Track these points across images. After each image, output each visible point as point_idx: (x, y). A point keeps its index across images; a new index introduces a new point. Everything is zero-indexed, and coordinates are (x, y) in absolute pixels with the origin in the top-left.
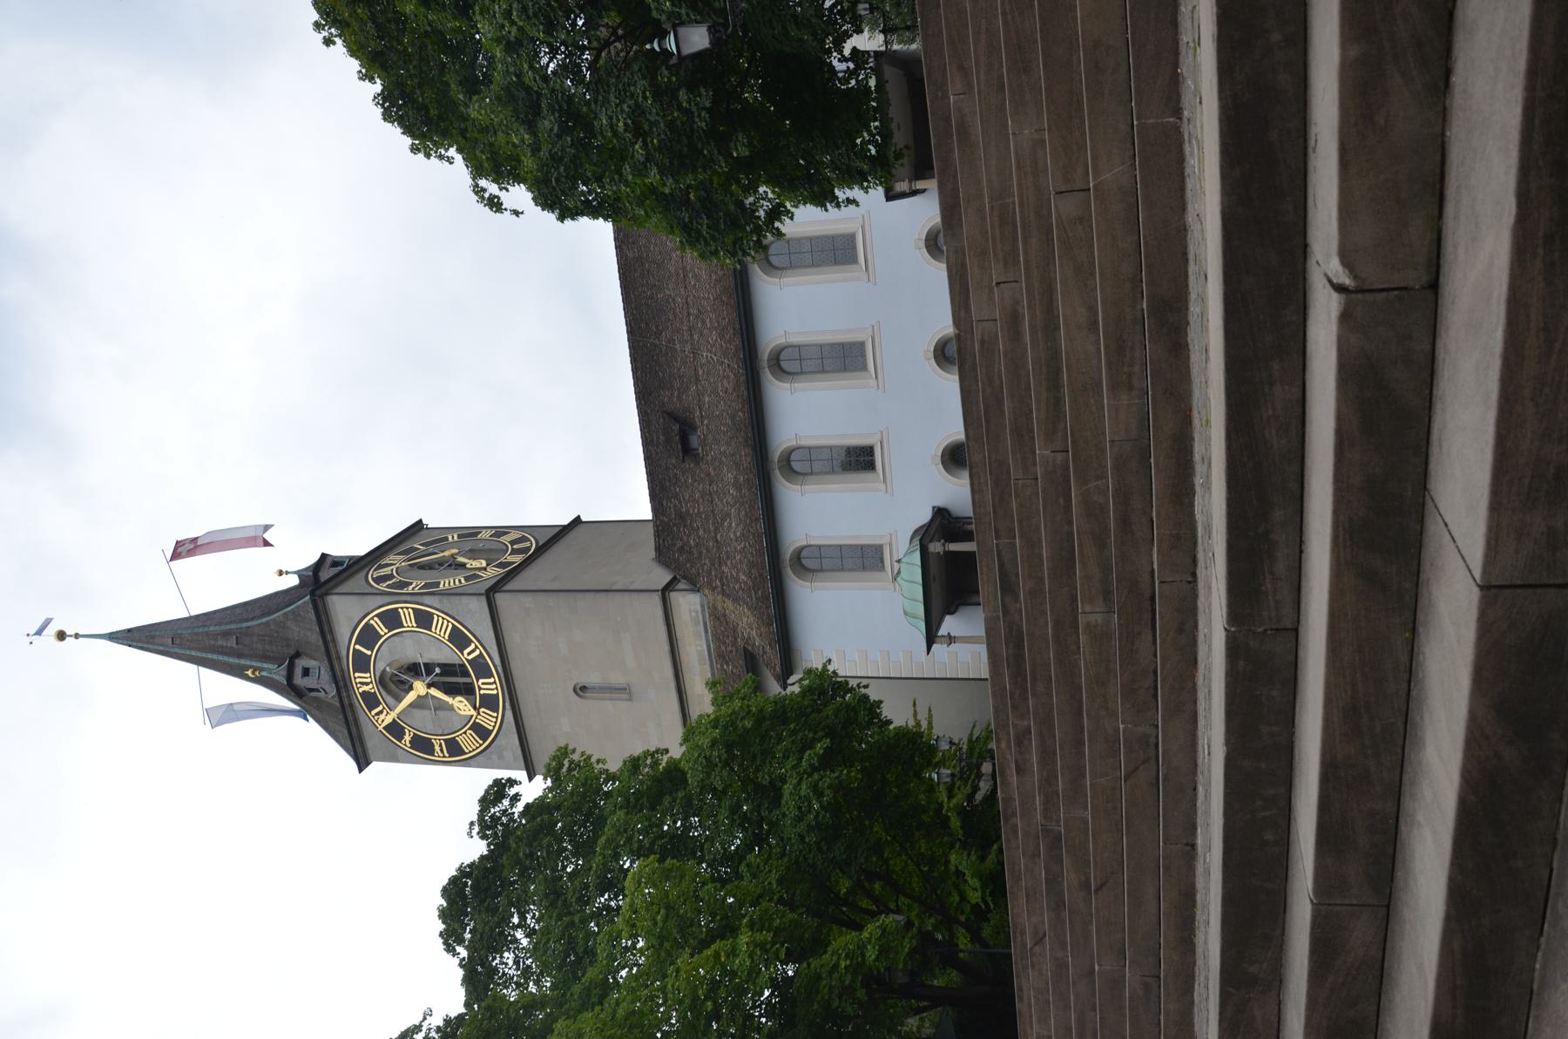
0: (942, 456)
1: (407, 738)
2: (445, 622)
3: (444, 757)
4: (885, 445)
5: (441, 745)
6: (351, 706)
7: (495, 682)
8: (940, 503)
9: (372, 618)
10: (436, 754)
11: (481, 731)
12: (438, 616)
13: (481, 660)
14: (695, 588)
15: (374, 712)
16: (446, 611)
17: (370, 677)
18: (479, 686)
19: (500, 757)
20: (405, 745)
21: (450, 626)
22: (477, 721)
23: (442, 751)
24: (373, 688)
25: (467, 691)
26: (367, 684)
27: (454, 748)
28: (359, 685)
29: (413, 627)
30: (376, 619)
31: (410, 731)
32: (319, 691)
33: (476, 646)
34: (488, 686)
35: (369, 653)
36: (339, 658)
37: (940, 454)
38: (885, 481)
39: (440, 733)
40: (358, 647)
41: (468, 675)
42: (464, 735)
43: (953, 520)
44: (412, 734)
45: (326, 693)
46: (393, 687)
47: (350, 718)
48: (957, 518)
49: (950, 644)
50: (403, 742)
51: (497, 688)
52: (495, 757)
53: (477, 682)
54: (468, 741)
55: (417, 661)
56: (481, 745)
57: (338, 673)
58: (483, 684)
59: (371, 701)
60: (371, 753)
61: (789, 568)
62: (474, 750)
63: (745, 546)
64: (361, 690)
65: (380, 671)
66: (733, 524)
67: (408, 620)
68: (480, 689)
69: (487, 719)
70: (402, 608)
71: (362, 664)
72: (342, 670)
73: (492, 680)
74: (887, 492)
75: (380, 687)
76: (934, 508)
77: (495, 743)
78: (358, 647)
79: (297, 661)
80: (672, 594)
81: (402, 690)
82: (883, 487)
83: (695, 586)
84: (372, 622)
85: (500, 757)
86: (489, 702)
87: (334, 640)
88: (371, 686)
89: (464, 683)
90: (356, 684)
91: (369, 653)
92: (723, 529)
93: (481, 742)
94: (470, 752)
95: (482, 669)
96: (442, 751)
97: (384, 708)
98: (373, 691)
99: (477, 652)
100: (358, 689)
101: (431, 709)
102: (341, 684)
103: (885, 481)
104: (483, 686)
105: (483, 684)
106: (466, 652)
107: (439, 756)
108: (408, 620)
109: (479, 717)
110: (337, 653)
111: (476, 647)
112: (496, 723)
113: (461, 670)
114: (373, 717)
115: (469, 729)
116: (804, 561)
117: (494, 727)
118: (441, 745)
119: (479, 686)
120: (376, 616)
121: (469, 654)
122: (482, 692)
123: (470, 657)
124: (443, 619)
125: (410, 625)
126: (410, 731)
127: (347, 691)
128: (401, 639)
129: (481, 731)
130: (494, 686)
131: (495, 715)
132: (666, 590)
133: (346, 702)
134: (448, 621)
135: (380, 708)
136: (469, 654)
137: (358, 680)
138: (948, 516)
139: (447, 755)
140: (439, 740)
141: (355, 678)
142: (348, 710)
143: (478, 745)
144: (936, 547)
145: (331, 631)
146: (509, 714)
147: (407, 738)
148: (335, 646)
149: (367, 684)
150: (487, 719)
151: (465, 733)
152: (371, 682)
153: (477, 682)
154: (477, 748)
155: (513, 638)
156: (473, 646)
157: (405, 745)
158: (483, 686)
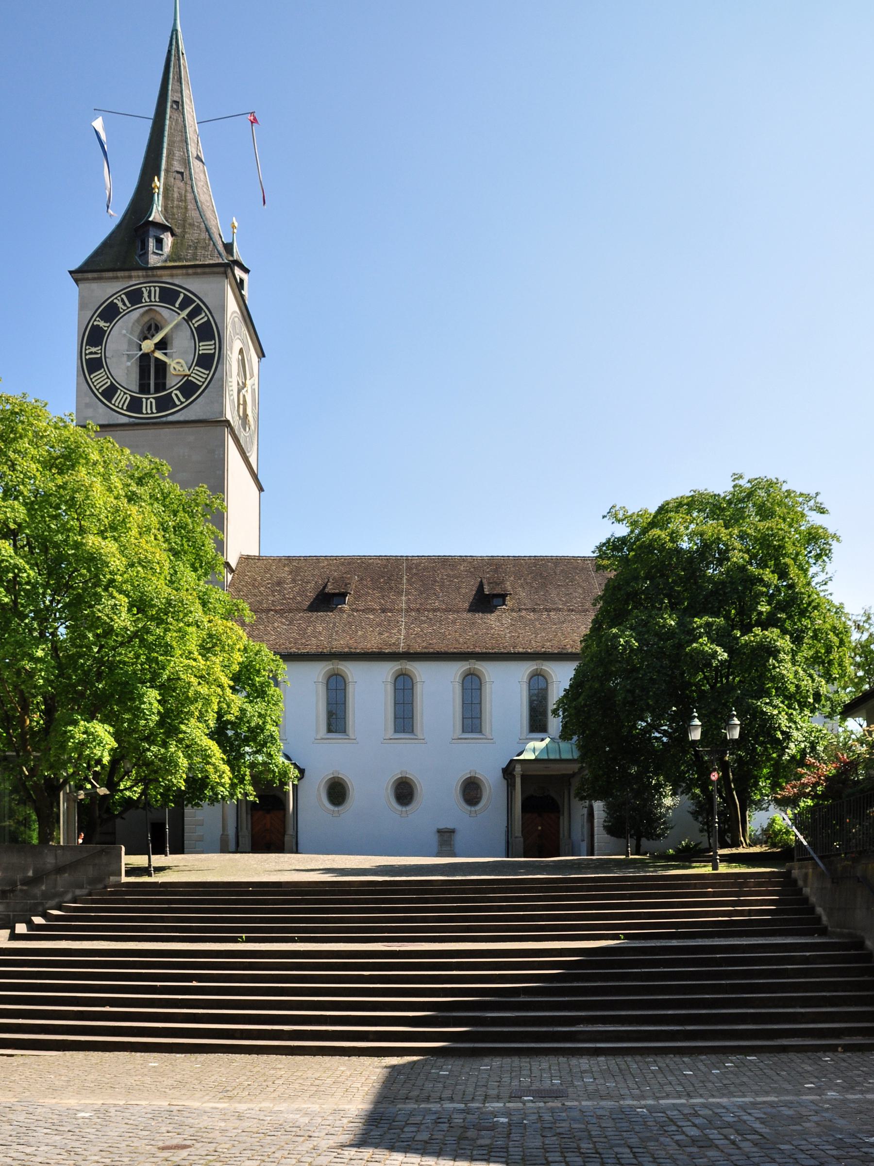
1: (102, 324)
2: (203, 380)
3: (86, 355)
5: (96, 353)
6: (130, 277)
7: (152, 413)
9: (206, 315)
10: (87, 347)
11: (110, 392)
12: (208, 375)
13: (171, 404)
15: (123, 296)
16: (213, 382)
17: (155, 301)
18: (149, 398)
19: (87, 405)
20: (95, 320)
21: (200, 384)
22: (119, 391)
23: (91, 353)
24: (146, 302)
25: (144, 388)
26: (149, 297)
27: (93, 365)
28: (148, 288)
29: (199, 350)
30: (206, 319)
31: (108, 327)
32: (142, 250)
33: (183, 403)
34: (149, 404)
35: (177, 305)
36: (172, 276)
38: (322, 739)
39: (107, 355)
40: (182, 296)
41: (156, 392)
42: (106, 377)
44: (106, 329)
45: (140, 256)
46: (146, 319)
47: (120, 274)
50: (98, 319)
51: (147, 413)
52: (87, 400)
53: (153, 398)
54: (100, 379)
55: (169, 347)
56: (98, 390)
57: (159, 272)
58: (151, 403)
59: (135, 297)
60: (85, 285)
62: (93, 383)
64: (144, 289)
65: (161, 312)
67: (206, 347)
68: (147, 399)
69: (121, 399)
70: (215, 344)
71: (168, 296)
72: (161, 276)
73: (154, 411)
75: (147, 308)
77: (100, 403)
78: (182, 296)
79: (169, 234)
81: (143, 327)
84: (203, 315)
85: (87, 405)
86: (135, 405)
87: (188, 274)
88: (148, 300)
89: (149, 384)
90: (150, 287)
91: (177, 305)
93: (100, 391)
94: (91, 379)
95: (165, 403)
96: (91, 353)
97: (128, 308)
98: (143, 301)
99: (178, 403)
100: (145, 287)
101: (127, 351)
102: (150, 273)
103: (322, 739)
104: (149, 401)
105: (151, 403)
106: (178, 392)
107: (86, 350)
108: (206, 347)
109: (122, 393)
110: (177, 275)
111: (182, 403)
112: (118, 407)
113: (161, 385)
114: (120, 296)
115: (111, 382)
117: (114, 405)
118: (96, 353)
119: (149, 398)
120: (208, 318)
121: (176, 395)
122: (144, 400)
123: (173, 395)
124: (206, 379)
125: (201, 348)
126: (108, 327)
127: (143, 277)
128: (189, 338)
129: (110, 392)
130: (149, 412)
131: (125, 408)
133: (134, 273)
134: (204, 383)
135: (129, 305)
136: (176, 395)
137: (152, 289)
139: (88, 357)
140: (101, 353)
141: (155, 287)
142: (127, 273)
143: (97, 387)
145: (195, 274)
146: (125, 420)
147: (102, 324)
148: (183, 275)
149: (149, 297)
150: (121, 399)
151: (108, 378)
152: (151, 301)
153: (153, 398)
154: (95, 386)
155: (189, 434)
156: (183, 400)
157: (95, 320)
158: (149, 401)
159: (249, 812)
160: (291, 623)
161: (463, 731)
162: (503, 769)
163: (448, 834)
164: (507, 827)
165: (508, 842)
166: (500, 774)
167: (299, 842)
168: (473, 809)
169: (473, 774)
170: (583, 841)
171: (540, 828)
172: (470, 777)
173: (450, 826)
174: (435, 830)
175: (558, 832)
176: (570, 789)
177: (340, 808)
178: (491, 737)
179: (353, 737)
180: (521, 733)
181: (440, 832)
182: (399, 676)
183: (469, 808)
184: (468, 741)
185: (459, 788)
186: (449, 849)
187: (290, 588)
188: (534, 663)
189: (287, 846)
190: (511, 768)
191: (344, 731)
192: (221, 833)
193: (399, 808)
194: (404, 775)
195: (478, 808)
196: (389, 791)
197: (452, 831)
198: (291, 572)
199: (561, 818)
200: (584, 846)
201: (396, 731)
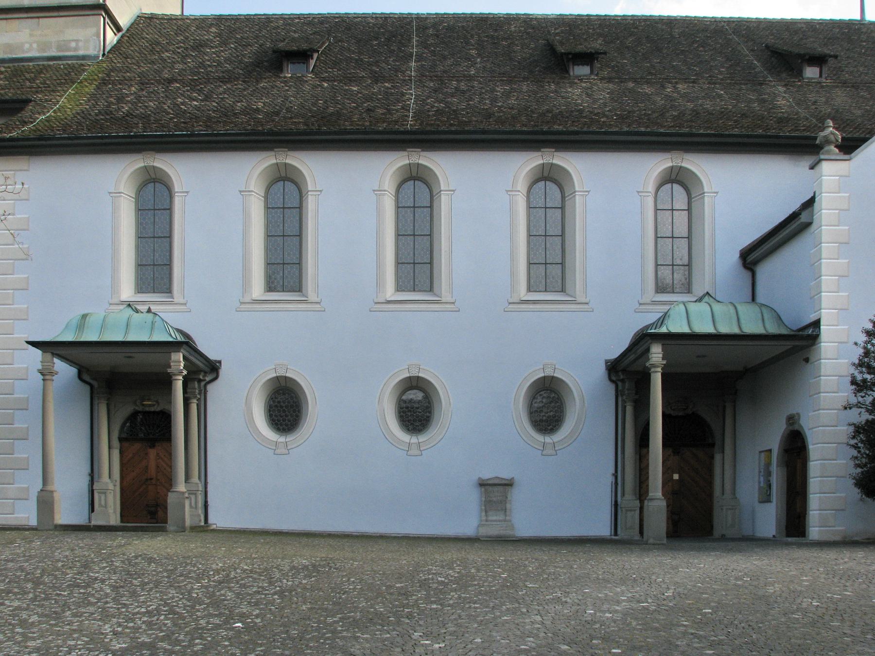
0: (286, 377)
4: (300, 306)
8: (224, 371)
37: (288, 375)
63: (169, 113)
66: (195, 103)
92: (188, 91)
159: (116, 443)
160: (207, 98)
161: (529, 290)
162: (607, 362)
163: (501, 488)
164: (615, 476)
165: (616, 505)
166: (601, 371)
168: (548, 439)
169: (549, 372)
170: (766, 498)
172: (544, 378)
173: (506, 475)
177: (290, 438)
178: (584, 300)
181: (483, 484)
183: (540, 438)
184: (538, 306)
185: (521, 399)
186: (502, 517)
191: (298, 287)
193: (405, 437)
194: (414, 373)
195: (558, 437)
197: (508, 484)
201: (399, 288)
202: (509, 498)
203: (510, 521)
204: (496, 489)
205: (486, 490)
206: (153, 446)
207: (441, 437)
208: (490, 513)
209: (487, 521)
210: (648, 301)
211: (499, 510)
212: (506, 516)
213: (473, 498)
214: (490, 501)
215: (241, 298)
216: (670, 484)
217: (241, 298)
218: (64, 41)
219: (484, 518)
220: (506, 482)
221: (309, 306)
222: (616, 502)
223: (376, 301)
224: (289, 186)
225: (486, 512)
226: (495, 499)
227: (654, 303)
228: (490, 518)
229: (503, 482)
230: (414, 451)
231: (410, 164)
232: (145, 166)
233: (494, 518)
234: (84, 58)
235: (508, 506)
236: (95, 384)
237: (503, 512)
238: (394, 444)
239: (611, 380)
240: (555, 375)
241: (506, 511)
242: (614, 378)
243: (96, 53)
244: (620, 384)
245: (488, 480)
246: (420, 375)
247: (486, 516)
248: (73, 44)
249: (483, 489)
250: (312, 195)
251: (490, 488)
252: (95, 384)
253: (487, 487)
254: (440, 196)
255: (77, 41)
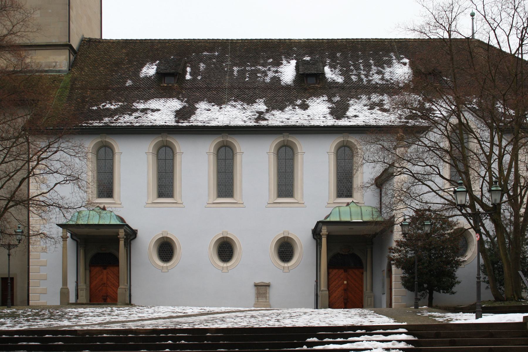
8: (139, 234)
14: (72, 65)
37: (168, 236)
43: (129, 240)
48: (130, 244)
49: (62, 238)
61: (100, 140)
74: (147, 204)
76: (137, 230)
80: (68, 51)
82: (150, 202)
83: (72, 67)
116: (103, 149)
132: (71, 47)
138: (131, 238)
144: (122, 233)
163: (264, 287)
165: (317, 295)
166: (311, 232)
167: (132, 294)
168: (286, 265)
169: (286, 235)
171: (345, 282)
173: (266, 281)
174: (253, 284)
175: (362, 286)
176: (372, 248)
179: (180, 202)
180: (329, 198)
181: (256, 285)
182: (221, 147)
183: (282, 264)
185: (273, 247)
186: (264, 300)
187: (127, 68)
188: (341, 135)
189: (120, 298)
190: (318, 230)
192: (61, 286)
194: (225, 235)
196: (212, 249)
197: (268, 286)
198: (127, 55)
199: (365, 273)
200: (384, 299)
202: (268, 292)
203: (269, 302)
204: (262, 287)
205: (257, 289)
206: (104, 269)
207: (237, 264)
208: (259, 299)
209: (258, 302)
210: (332, 202)
211: (263, 297)
212: (266, 300)
213: (252, 291)
214: (260, 293)
215: (147, 202)
216: (343, 286)
217: (147, 202)
218: (49, 62)
219: (257, 301)
220: (267, 284)
221: (178, 205)
222: (317, 294)
223: (208, 203)
224: (168, 149)
225: (257, 298)
226: (261, 292)
227: (334, 203)
228: (259, 301)
229: (265, 284)
230: (225, 270)
231: (223, 140)
232: (102, 141)
233: (261, 301)
234: (59, 71)
235: (268, 295)
236: (79, 240)
237: (265, 298)
238: (216, 267)
239: (314, 238)
240: (289, 236)
241: (266, 298)
242: (315, 237)
243: (66, 69)
244: (318, 240)
245: (258, 283)
246: (228, 236)
247: (258, 300)
248: (54, 64)
249: (256, 288)
250: (178, 155)
251: (259, 287)
252: (79, 240)
253: (258, 287)
254: (237, 155)
255: (56, 62)
